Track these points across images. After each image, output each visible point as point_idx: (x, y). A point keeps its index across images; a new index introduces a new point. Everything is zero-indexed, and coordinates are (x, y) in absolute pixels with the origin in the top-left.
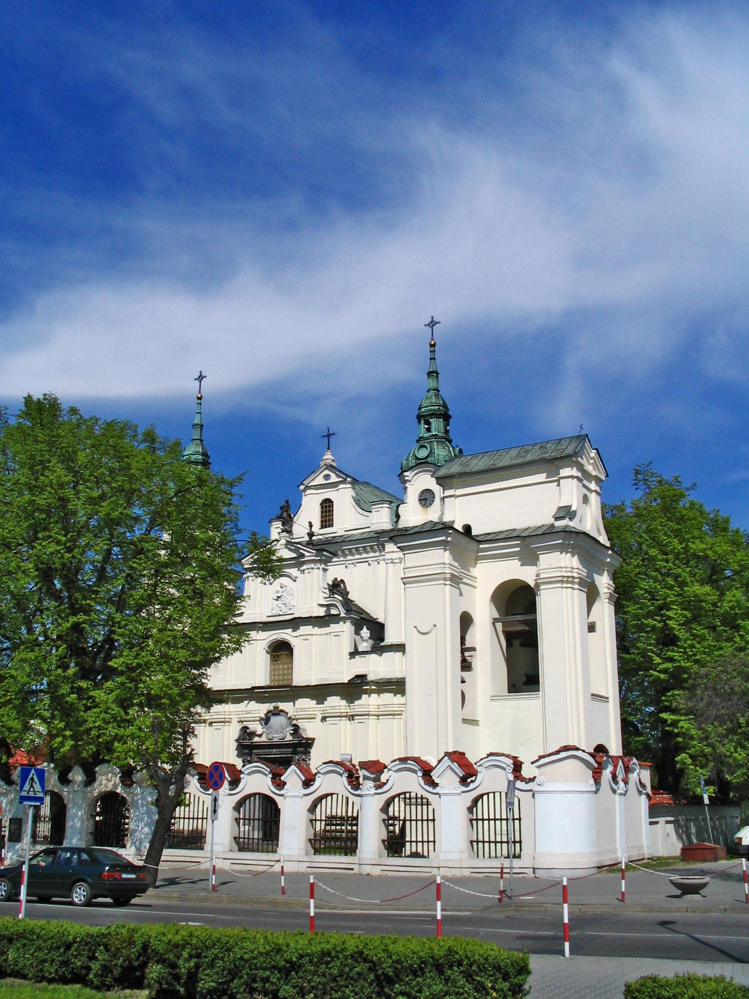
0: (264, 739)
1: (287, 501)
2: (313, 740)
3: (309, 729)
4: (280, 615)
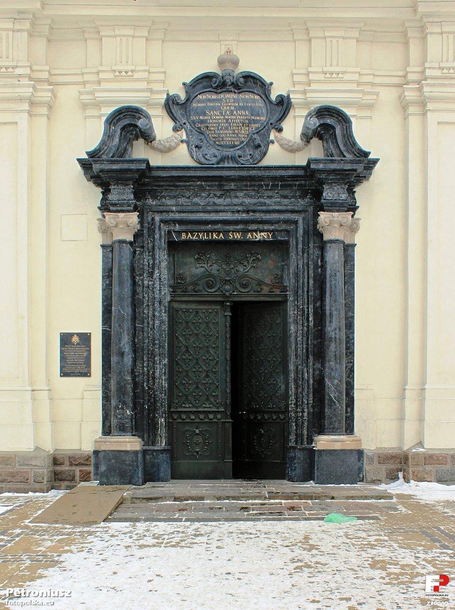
0: (182, 157)
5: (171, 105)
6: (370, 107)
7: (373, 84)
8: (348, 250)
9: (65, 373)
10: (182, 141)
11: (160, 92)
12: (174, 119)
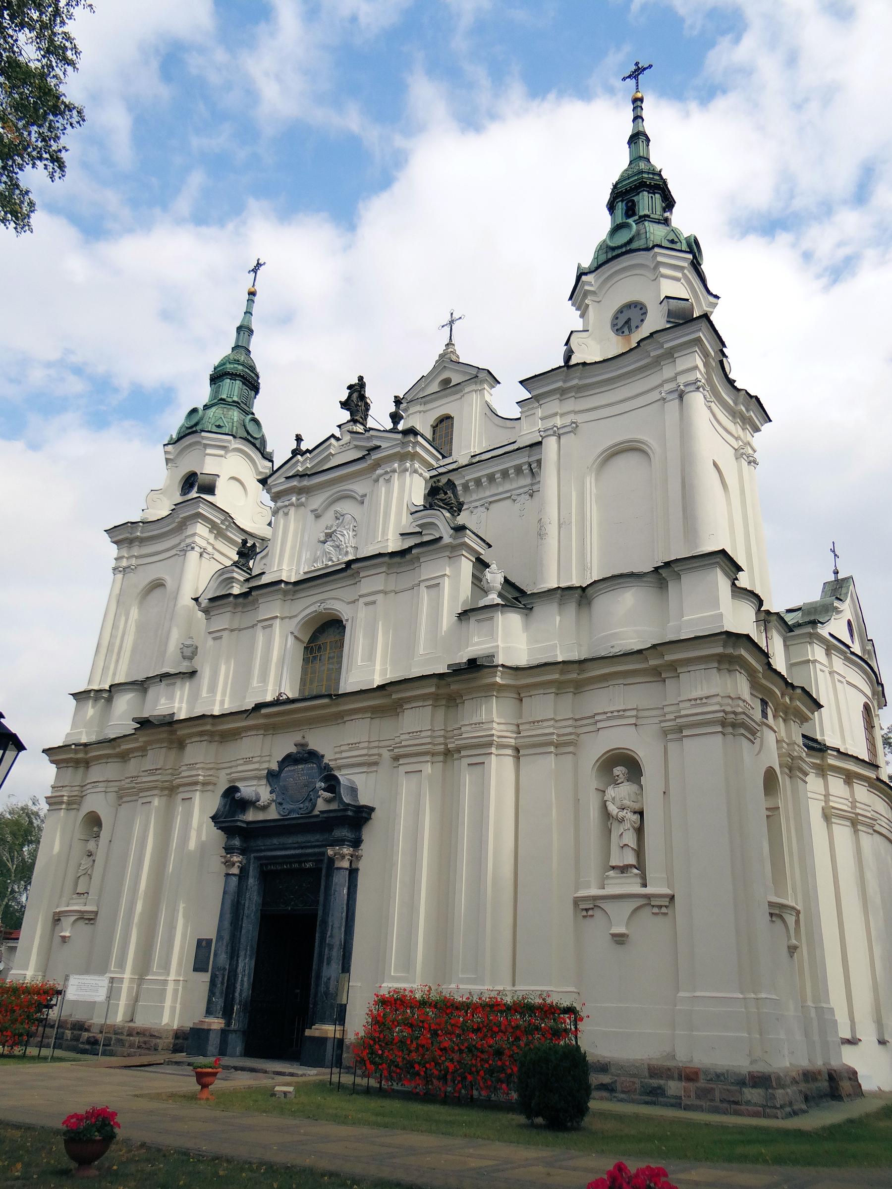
0: (273, 814)
1: (361, 378)
2: (372, 809)
3: (365, 787)
4: (327, 567)
5: (272, 776)
6: (376, 764)
7: (379, 747)
8: (353, 873)
9: (196, 969)
10: (273, 801)
11: (263, 769)
12: (271, 786)
